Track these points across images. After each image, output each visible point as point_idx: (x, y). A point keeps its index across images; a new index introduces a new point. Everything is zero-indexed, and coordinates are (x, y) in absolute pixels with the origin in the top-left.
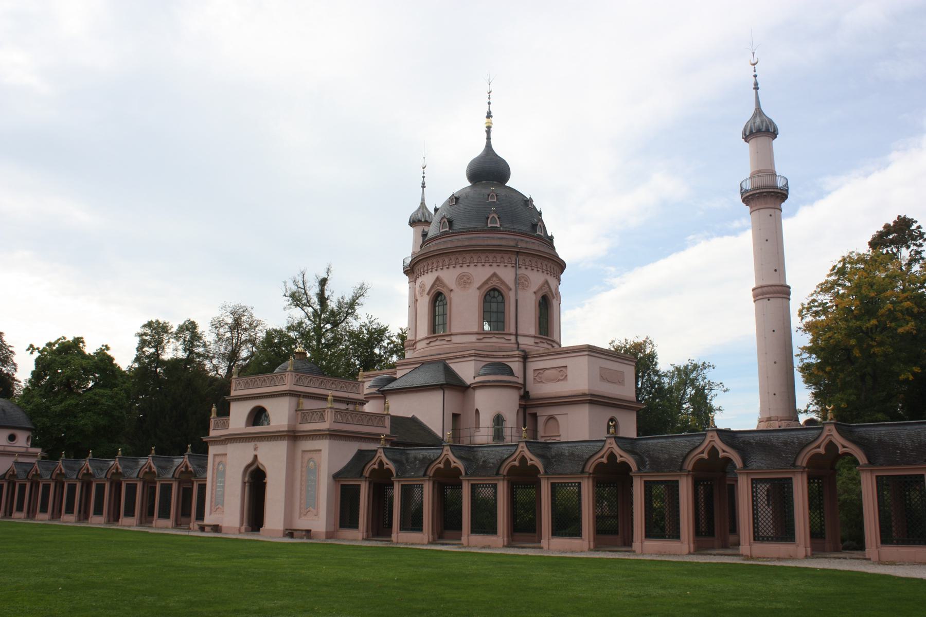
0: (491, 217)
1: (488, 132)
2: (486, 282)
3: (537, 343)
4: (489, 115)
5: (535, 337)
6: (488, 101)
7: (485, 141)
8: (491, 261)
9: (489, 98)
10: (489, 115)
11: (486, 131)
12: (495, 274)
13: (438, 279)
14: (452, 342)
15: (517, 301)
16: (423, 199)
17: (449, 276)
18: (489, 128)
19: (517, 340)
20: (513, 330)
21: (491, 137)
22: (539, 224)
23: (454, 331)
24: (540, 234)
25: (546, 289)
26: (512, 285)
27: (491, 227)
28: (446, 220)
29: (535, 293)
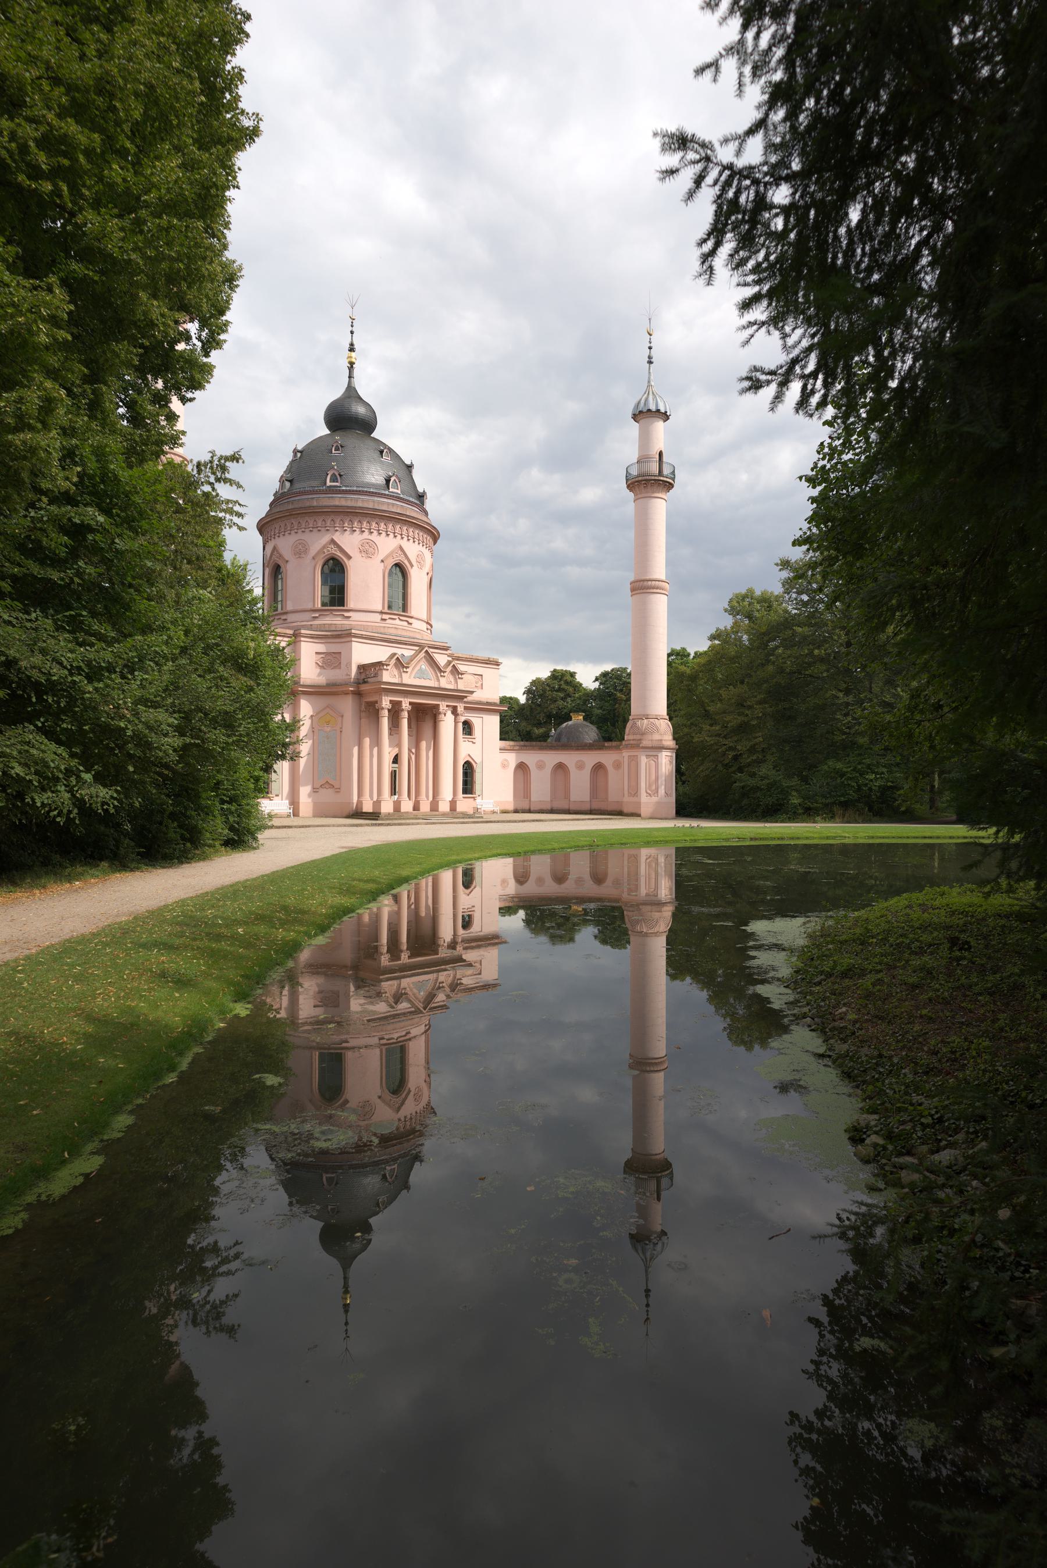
0: (330, 473)
3: (385, 620)
4: (352, 349)
5: (382, 613)
6: (351, 328)
8: (328, 524)
9: (352, 326)
10: (352, 349)
12: (333, 541)
13: (275, 549)
14: (289, 621)
17: (285, 544)
18: (352, 364)
22: (392, 479)
23: (290, 607)
24: (396, 491)
25: (399, 558)
27: (331, 486)
29: (382, 561)
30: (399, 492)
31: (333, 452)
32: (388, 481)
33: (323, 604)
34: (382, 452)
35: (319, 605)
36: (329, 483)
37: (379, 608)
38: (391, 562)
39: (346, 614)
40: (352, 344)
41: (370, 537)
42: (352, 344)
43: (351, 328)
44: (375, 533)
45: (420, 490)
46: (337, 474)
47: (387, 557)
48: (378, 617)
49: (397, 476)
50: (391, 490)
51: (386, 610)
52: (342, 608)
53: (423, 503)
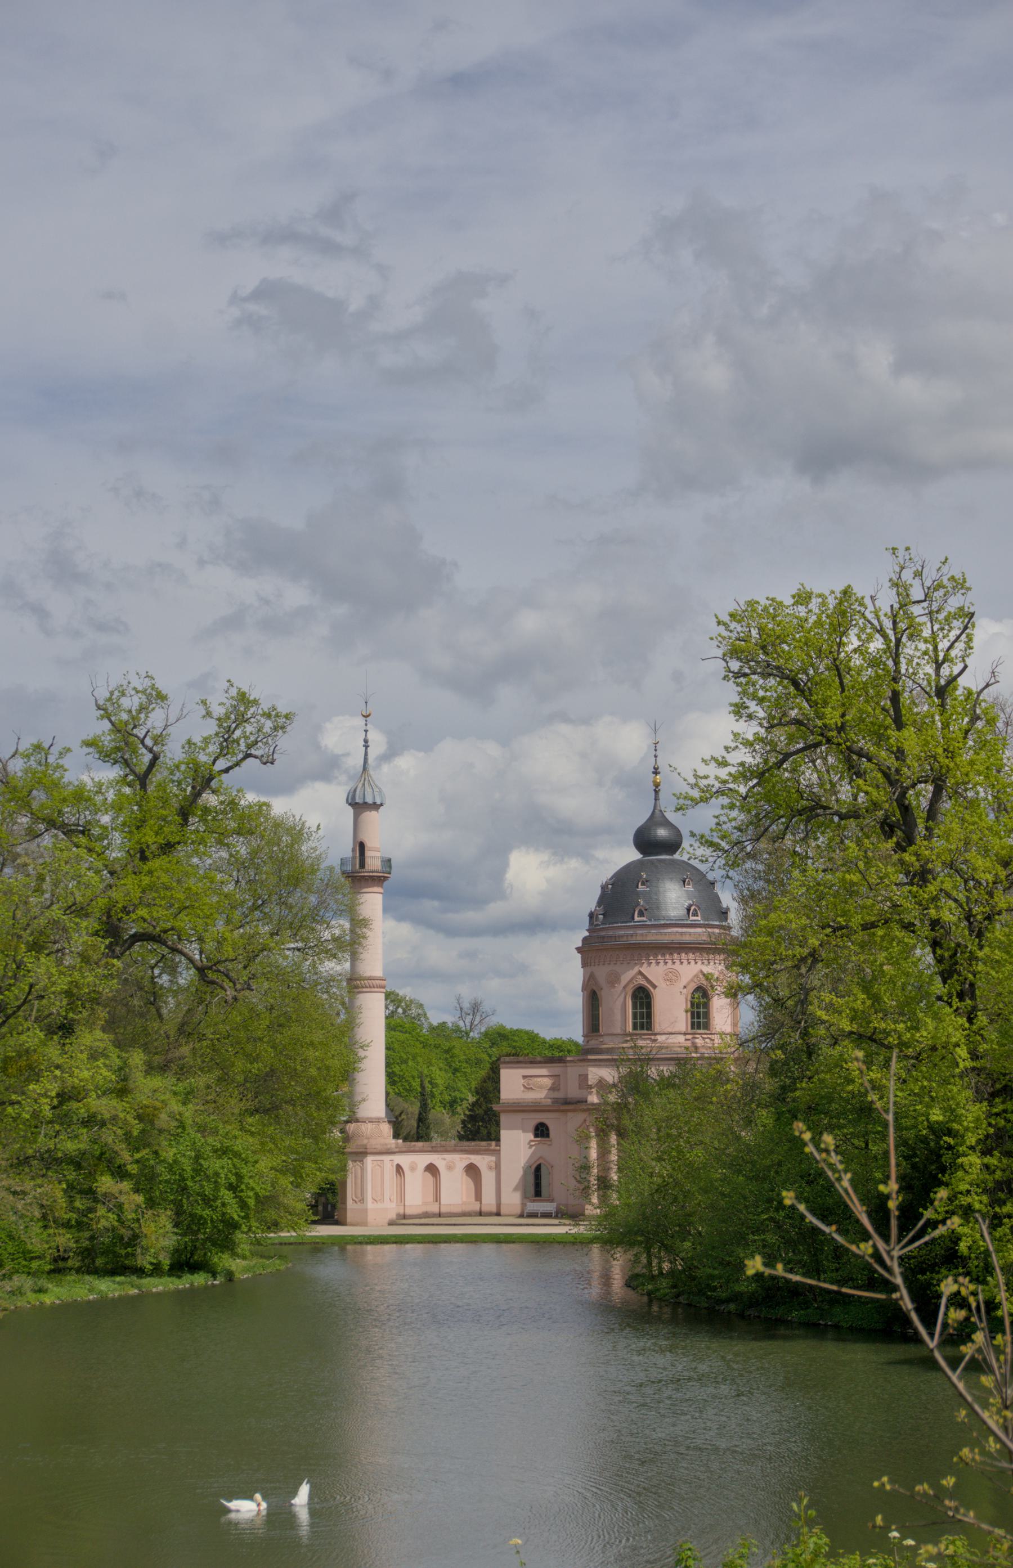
1: (656, 792)
4: (656, 772)
6: (654, 753)
12: (640, 973)
17: (602, 972)
18: (657, 785)
22: (693, 908)
30: (699, 918)
31: (640, 886)
32: (688, 910)
33: (635, 1027)
34: (684, 882)
35: (630, 1028)
36: (636, 918)
37: (683, 1029)
38: (693, 986)
39: (653, 1037)
41: (674, 967)
43: (654, 753)
44: (678, 962)
45: (725, 906)
46: (643, 909)
47: (688, 983)
48: (681, 1039)
49: (696, 905)
50: (692, 918)
51: (689, 1030)
52: (650, 1032)
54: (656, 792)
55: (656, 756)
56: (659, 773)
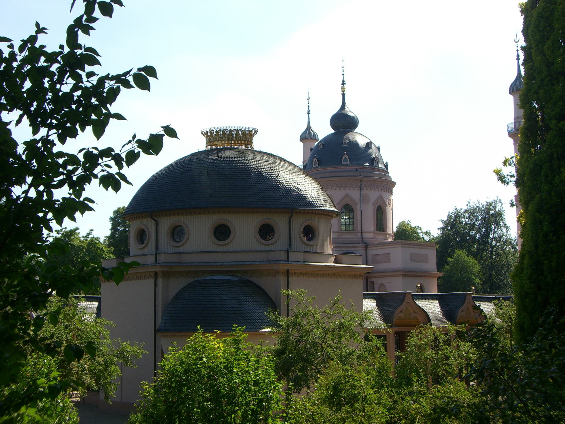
0: (344, 157)
1: (343, 95)
2: (342, 200)
4: (343, 83)
7: (342, 100)
9: (343, 71)
10: (343, 83)
11: (342, 94)
12: (347, 195)
15: (361, 211)
16: (309, 123)
18: (343, 92)
19: (362, 234)
20: (359, 229)
21: (345, 98)
26: (358, 201)
28: (316, 160)
36: (343, 163)
40: (343, 81)
42: (343, 81)
53: (387, 168)
54: (343, 95)
55: (343, 75)
56: (345, 84)
